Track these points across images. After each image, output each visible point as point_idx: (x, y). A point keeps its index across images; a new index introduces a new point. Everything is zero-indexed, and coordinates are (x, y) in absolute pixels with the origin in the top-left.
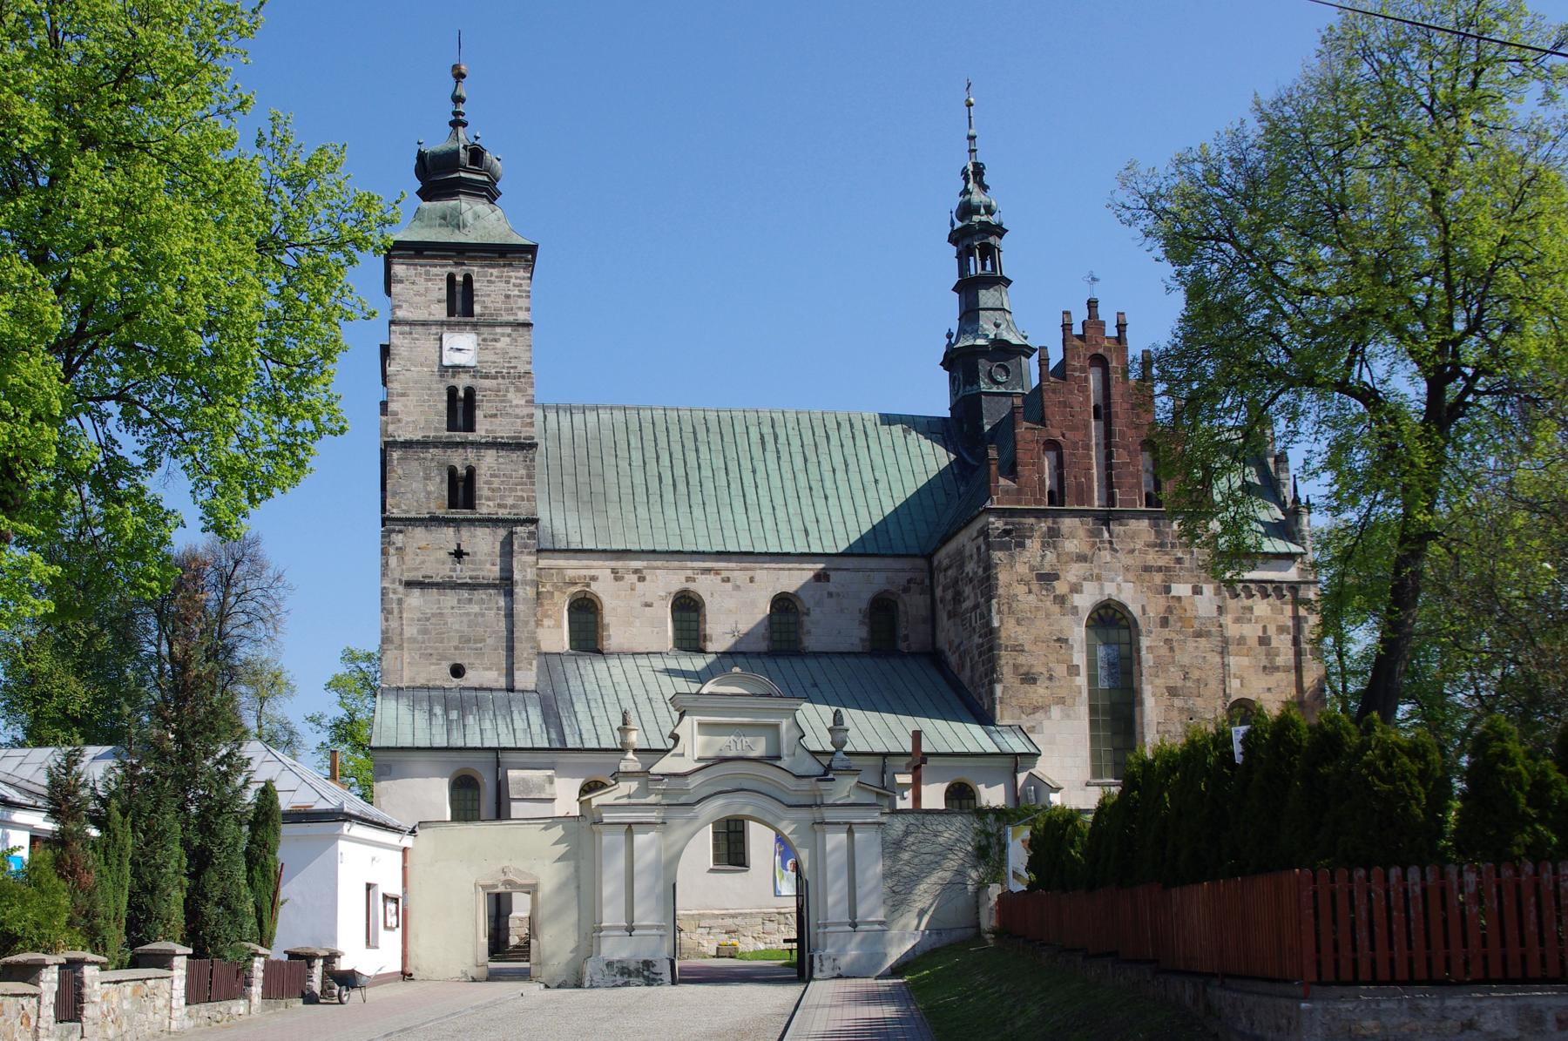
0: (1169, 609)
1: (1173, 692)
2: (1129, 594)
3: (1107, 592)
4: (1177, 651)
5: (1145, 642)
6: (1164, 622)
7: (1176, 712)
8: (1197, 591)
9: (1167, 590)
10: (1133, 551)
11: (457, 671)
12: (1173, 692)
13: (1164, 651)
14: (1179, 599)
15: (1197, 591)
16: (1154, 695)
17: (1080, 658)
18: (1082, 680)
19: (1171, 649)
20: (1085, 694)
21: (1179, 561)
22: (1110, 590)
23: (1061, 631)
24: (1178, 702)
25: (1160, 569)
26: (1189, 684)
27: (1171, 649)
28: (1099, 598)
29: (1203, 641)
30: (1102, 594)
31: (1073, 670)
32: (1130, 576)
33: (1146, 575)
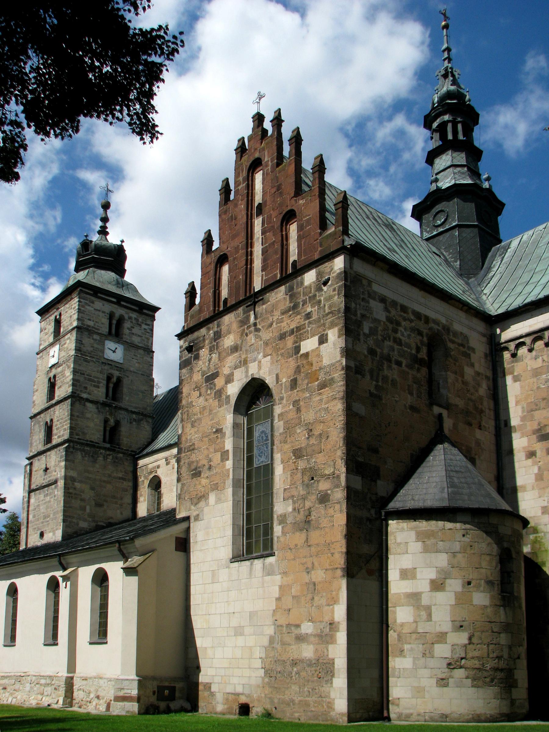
0: (298, 370)
1: (298, 454)
2: (264, 368)
3: (250, 373)
4: (303, 410)
5: (278, 410)
6: (294, 384)
7: (299, 475)
8: (323, 340)
9: (297, 349)
10: (272, 324)
11: (42, 535)
12: (298, 454)
13: (292, 415)
14: (307, 355)
15: (323, 340)
17: (229, 445)
18: (229, 464)
19: (299, 410)
20: (231, 477)
21: (308, 316)
22: (253, 370)
23: (218, 423)
24: (302, 464)
25: (292, 332)
26: (313, 441)
27: (299, 410)
28: (245, 381)
29: (327, 392)
30: (247, 376)
31: (224, 455)
32: (269, 350)
33: (281, 344)
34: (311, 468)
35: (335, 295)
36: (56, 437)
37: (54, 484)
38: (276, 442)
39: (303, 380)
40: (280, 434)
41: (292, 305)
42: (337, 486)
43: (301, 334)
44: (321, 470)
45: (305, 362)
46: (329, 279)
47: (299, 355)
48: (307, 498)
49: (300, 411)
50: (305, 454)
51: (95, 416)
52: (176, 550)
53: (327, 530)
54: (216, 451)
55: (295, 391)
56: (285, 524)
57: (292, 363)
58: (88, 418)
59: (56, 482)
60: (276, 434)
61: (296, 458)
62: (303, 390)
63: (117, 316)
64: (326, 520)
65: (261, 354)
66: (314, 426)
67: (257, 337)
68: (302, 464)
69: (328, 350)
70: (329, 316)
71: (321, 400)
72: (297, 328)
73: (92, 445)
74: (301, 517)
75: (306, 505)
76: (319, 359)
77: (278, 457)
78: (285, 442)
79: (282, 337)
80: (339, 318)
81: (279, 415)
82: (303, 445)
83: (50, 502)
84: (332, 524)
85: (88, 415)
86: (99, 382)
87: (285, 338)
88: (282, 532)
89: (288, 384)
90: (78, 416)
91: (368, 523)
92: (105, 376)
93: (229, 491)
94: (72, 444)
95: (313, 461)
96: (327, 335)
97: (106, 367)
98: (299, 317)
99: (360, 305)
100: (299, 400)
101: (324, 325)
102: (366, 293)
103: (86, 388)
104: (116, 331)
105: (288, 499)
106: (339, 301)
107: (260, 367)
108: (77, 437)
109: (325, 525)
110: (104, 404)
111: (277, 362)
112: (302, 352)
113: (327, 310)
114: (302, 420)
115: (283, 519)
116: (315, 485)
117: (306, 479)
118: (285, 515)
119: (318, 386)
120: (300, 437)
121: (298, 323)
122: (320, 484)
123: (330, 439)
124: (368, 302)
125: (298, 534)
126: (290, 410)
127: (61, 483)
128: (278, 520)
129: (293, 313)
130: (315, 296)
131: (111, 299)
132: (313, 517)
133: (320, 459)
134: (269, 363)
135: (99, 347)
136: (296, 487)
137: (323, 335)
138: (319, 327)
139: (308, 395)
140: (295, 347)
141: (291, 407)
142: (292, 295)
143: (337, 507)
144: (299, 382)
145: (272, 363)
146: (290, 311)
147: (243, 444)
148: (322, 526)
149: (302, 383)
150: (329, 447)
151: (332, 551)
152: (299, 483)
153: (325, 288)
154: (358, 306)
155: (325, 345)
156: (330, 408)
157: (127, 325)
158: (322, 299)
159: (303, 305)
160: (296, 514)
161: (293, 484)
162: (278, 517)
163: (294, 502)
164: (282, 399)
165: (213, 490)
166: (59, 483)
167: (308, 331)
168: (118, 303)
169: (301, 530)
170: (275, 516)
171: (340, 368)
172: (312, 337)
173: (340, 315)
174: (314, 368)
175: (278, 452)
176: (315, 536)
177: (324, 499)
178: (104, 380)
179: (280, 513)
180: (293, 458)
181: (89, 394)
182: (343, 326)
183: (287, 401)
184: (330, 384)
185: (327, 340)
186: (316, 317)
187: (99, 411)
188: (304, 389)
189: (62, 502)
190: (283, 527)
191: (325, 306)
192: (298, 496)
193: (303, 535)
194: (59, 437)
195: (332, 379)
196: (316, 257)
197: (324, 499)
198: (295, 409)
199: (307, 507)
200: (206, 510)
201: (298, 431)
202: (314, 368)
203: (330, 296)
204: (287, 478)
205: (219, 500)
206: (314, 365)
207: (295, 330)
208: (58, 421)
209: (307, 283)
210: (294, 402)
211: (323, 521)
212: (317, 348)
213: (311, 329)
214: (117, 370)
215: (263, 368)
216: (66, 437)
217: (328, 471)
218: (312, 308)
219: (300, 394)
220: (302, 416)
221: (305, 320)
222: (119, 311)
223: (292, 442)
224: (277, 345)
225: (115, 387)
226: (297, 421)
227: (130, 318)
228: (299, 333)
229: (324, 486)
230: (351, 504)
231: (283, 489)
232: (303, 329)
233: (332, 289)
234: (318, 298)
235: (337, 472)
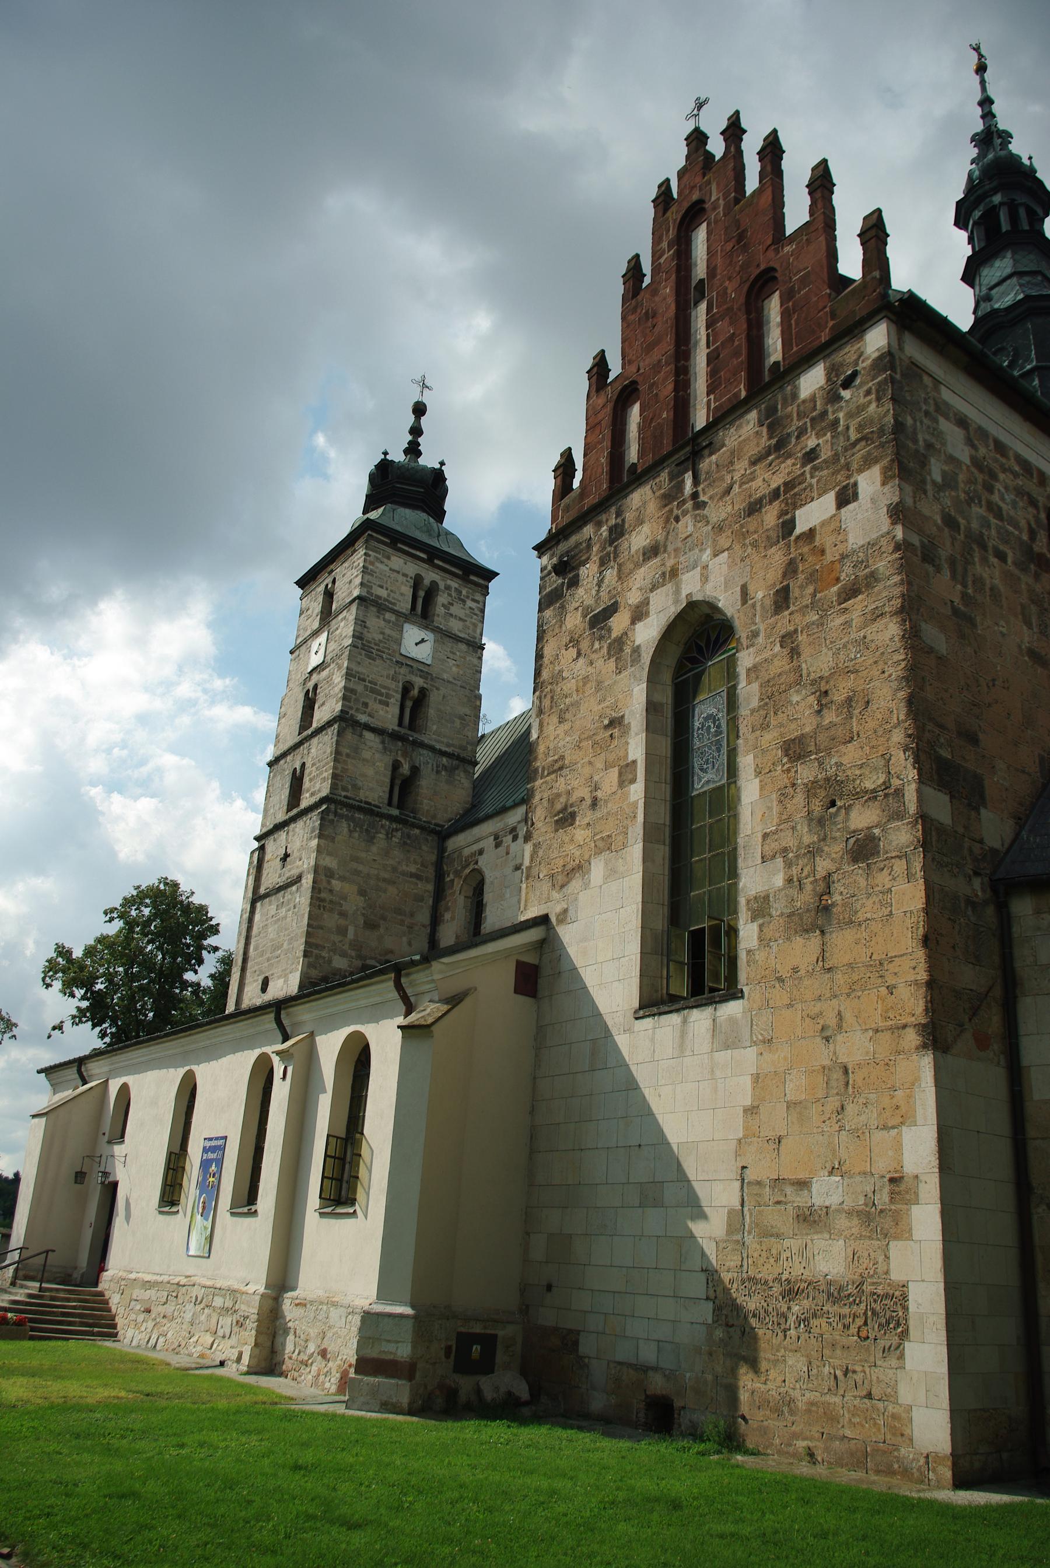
0: (791, 569)
1: (795, 750)
4: (806, 652)
5: (745, 660)
6: (782, 599)
7: (800, 799)
9: (788, 526)
10: (728, 490)
12: (795, 750)
13: (781, 664)
14: (810, 534)
16: (758, 773)
17: (636, 749)
20: (640, 818)
22: (691, 586)
24: (806, 773)
25: (775, 494)
26: (830, 716)
27: (795, 653)
28: (673, 610)
32: (724, 541)
33: (752, 523)
34: (827, 779)
35: (870, 402)
36: (308, 795)
37: (296, 883)
38: (743, 729)
39: (801, 587)
40: (753, 711)
41: (774, 441)
42: (898, 816)
43: (795, 495)
44: (854, 780)
45: (805, 549)
46: (855, 374)
47: (792, 538)
48: (820, 850)
49: (799, 655)
50: (812, 748)
51: (377, 756)
52: (515, 992)
53: (875, 926)
54: (607, 766)
55: (787, 613)
56: (767, 919)
57: (777, 557)
58: (364, 760)
59: (299, 878)
60: (744, 711)
61: (790, 761)
62: (803, 610)
63: (427, 582)
64: (871, 901)
65: (708, 552)
66: (832, 683)
67: (697, 519)
68: (806, 773)
69: (860, 517)
70: (858, 447)
71: (847, 624)
72: (786, 484)
73: (369, 810)
74: (806, 898)
75: (818, 869)
76: (840, 538)
77: (746, 762)
78: (765, 726)
79: (754, 508)
80: (882, 445)
81: (749, 670)
82: (807, 729)
83: (285, 917)
84: (887, 912)
85: (366, 754)
86: (388, 696)
87: (759, 510)
88: (761, 939)
89: (768, 602)
90: (348, 755)
91: (970, 913)
92: (401, 685)
93: (636, 851)
94: (333, 807)
95: (833, 761)
96: (855, 484)
97: (404, 670)
98: (789, 462)
99: (921, 422)
100: (796, 631)
101: (847, 466)
102: (931, 402)
103: (366, 705)
104: (423, 607)
105: (774, 857)
106: (879, 412)
107: (705, 579)
108: (344, 794)
109: (869, 915)
110: (395, 736)
111: (742, 560)
112: (798, 531)
113: (853, 435)
114: (804, 672)
115: (761, 908)
116: (840, 819)
117: (817, 806)
118: (766, 898)
119: (839, 595)
120: (801, 713)
121: (789, 474)
122: (853, 814)
123: (873, 707)
124: (937, 422)
125: (799, 940)
126: (775, 656)
127: (307, 881)
128: (748, 909)
129: (777, 458)
130: (824, 414)
131: (418, 553)
132: (837, 898)
133: (850, 755)
134: (725, 567)
135: (393, 634)
136: (793, 828)
137: (846, 487)
138: (835, 473)
139: (817, 617)
140: (783, 523)
141: (777, 648)
142: (772, 422)
143: (900, 866)
144: (795, 592)
145: (732, 565)
146: (769, 454)
147: (665, 746)
148: (861, 916)
149: (802, 594)
150: (871, 724)
151: (891, 980)
152: (799, 816)
153: (846, 394)
154: (918, 424)
155: (851, 507)
156: (869, 638)
157: (442, 599)
158: (841, 415)
159: (798, 438)
160: (794, 892)
161: (786, 819)
162: (748, 902)
163: (788, 864)
164: (755, 634)
165: (599, 851)
166: (304, 881)
167: (811, 485)
168: (430, 561)
169: (807, 931)
170: (742, 901)
171: (891, 549)
172: (820, 496)
173: (883, 439)
174: (829, 557)
175: (747, 752)
176: (844, 944)
177: (864, 850)
178: (397, 692)
179: (753, 892)
180: (785, 760)
181: (370, 715)
182: (892, 461)
183: (768, 637)
184: (868, 586)
185: (855, 497)
186: (829, 454)
187: (385, 748)
188: (807, 606)
189: (306, 915)
190: (761, 926)
191: (848, 428)
192: (799, 848)
193: (815, 940)
194: (312, 794)
195: (872, 574)
196: (824, 337)
197: (864, 850)
198: (786, 651)
199: (821, 872)
200: (583, 897)
201: (795, 698)
202: (829, 557)
203: (858, 407)
204: (770, 808)
205: (612, 874)
206: (828, 551)
207: (782, 489)
208: (313, 765)
209: (805, 392)
210: (783, 637)
211: (863, 905)
212: (834, 515)
213: (818, 482)
214: (421, 677)
215: (712, 578)
216: (325, 792)
217: (872, 782)
218: (818, 438)
219: (797, 618)
220: (804, 665)
221: (803, 465)
222: (430, 576)
223: (781, 725)
224: (742, 526)
225: (415, 704)
226: (792, 677)
227: (448, 588)
228: (791, 495)
229: (862, 818)
230: (933, 859)
231: (760, 835)
232: (800, 484)
233: (862, 391)
234: (831, 417)
235: (895, 782)
